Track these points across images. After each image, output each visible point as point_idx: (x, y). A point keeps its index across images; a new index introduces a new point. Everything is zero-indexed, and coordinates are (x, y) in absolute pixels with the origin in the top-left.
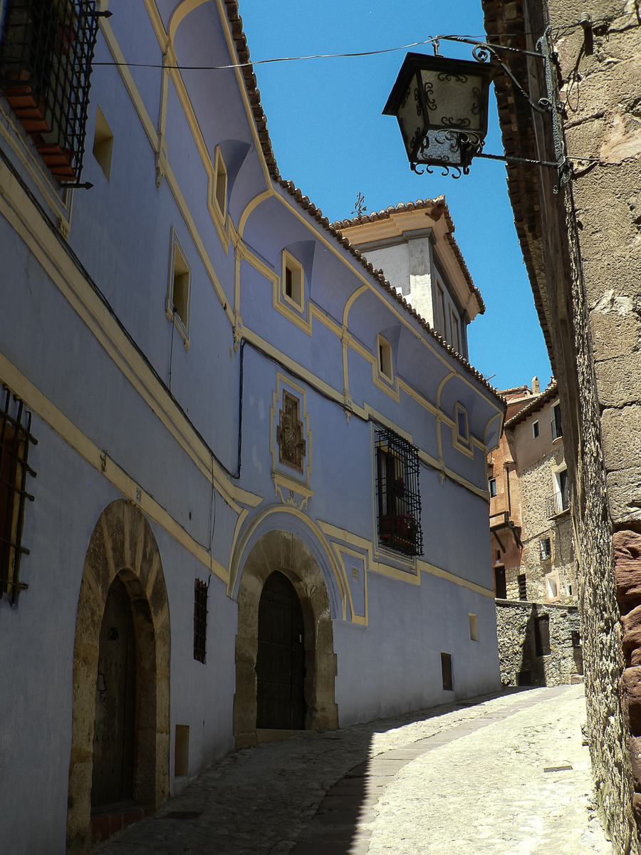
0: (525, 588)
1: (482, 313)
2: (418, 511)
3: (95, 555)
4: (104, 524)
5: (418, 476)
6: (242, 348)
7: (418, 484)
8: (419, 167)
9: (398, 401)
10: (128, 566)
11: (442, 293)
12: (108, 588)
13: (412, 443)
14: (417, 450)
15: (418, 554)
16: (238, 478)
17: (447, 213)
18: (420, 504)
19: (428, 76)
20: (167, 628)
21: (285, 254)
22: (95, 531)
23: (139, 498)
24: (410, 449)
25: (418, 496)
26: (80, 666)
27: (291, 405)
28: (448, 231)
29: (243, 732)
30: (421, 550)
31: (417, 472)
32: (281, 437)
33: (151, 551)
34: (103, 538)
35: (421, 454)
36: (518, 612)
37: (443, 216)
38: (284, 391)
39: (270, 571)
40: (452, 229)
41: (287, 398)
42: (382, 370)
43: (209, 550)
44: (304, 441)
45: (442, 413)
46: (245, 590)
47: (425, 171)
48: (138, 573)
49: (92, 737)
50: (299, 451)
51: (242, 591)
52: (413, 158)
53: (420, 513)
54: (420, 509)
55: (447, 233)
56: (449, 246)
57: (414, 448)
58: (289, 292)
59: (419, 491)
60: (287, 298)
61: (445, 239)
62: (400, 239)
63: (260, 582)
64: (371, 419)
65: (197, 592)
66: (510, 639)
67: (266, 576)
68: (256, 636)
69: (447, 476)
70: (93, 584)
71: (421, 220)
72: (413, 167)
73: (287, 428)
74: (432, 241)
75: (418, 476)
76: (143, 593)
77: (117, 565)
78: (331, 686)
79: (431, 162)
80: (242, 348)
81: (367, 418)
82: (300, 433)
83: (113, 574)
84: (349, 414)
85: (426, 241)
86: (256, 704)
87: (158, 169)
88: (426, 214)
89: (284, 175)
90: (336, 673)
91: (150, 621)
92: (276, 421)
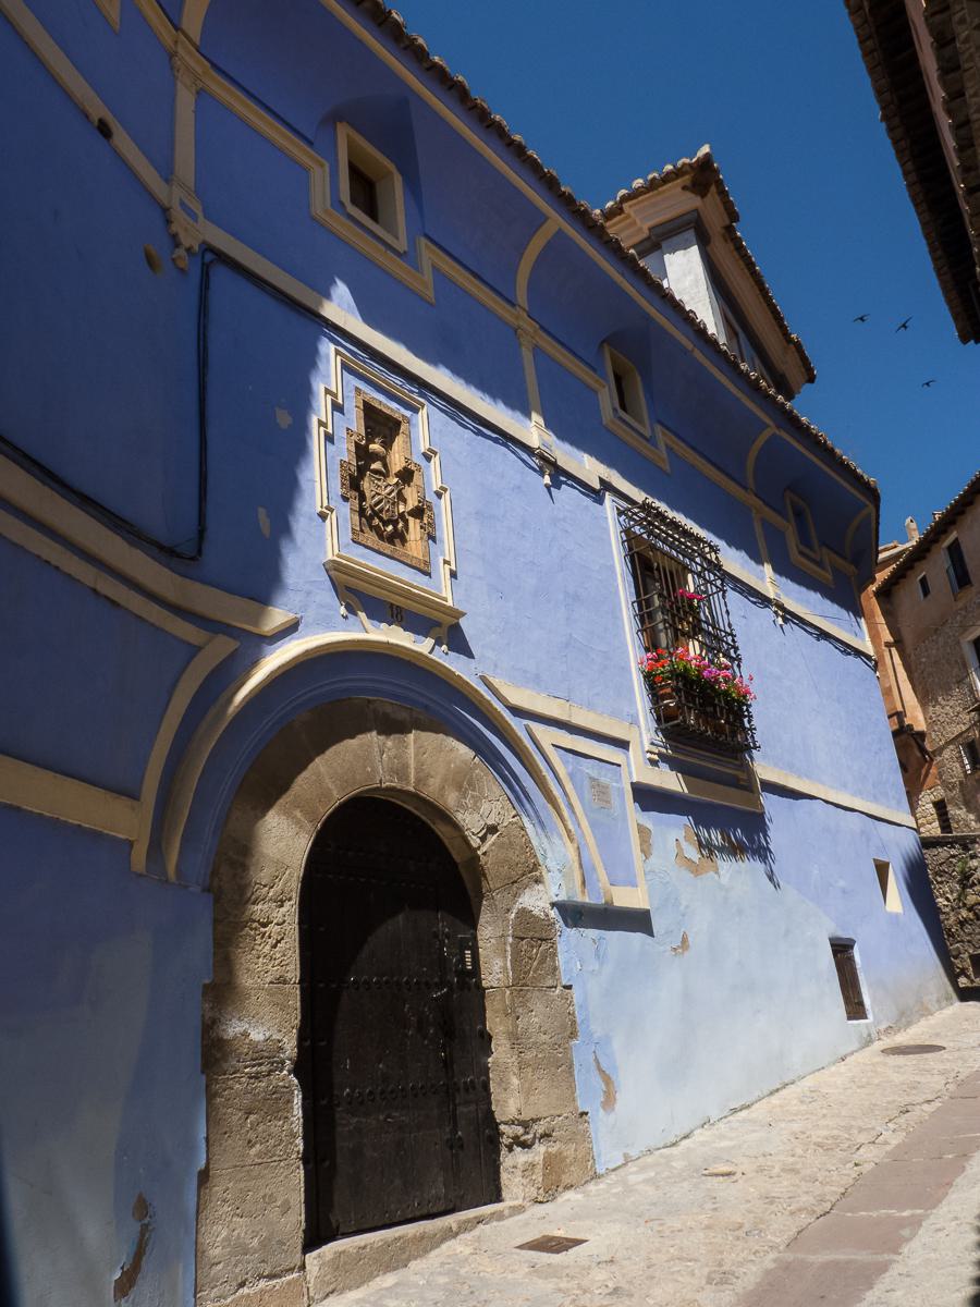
0: (948, 820)
1: (811, 379)
5: (724, 597)
7: (728, 612)
9: (667, 468)
11: (736, 334)
17: (719, 183)
18: (736, 649)
21: (343, 132)
25: (731, 634)
28: (727, 222)
29: (242, 1285)
30: (752, 737)
36: (953, 852)
37: (713, 189)
38: (358, 390)
42: (623, 407)
45: (761, 503)
56: (735, 253)
61: (726, 241)
63: (298, 822)
64: (607, 486)
66: (948, 899)
67: (326, 811)
68: (293, 972)
71: (677, 201)
74: (704, 242)
81: (597, 486)
88: (684, 188)
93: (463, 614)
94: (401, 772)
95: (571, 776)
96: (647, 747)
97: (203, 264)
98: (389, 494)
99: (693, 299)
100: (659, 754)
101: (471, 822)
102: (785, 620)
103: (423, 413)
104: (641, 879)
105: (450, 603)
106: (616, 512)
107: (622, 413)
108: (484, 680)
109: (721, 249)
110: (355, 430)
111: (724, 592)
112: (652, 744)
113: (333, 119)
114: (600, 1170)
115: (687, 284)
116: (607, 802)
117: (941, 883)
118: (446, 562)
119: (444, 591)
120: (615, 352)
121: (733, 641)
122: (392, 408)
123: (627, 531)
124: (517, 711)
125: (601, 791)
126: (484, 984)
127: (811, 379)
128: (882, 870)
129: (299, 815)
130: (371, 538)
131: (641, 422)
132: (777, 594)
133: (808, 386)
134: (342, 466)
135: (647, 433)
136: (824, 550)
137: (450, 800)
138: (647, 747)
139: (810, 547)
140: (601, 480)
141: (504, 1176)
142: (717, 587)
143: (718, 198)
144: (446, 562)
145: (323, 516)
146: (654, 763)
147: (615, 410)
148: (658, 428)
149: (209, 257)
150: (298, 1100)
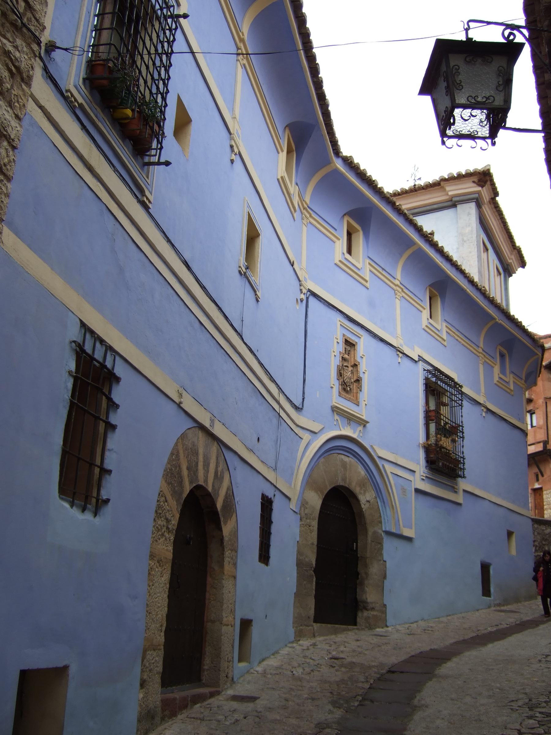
2: (461, 439)
3: (172, 474)
4: (180, 447)
6: (307, 298)
7: (462, 416)
8: (450, 142)
10: (201, 483)
11: (487, 250)
12: (182, 502)
13: (456, 380)
14: (461, 387)
15: (461, 477)
16: (302, 409)
18: (463, 433)
19: (455, 60)
20: (235, 533)
22: (172, 454)
23: (212, 425)
24: (456, 386)
26: (155, 567)
27: (349, 344)
28: (493, 196)
29: (301, 625)
30: (463, 473)
31: (461, 405)
32: (340, 374)
33: (222, 469)
34: (179, 460)
35: (465, 390)
37: (489, 183)
38: (344, 335)
39: (329, 488)
40: (496, 194)
41: (346, 341)
42: (431, 317)
43: (275, 470)
44: (361, 378)
46: (307, 503)
47: (455, 145)
48: (210, 489)
49: (164, 629)
50: (357, 386)
51: (304, 504)
52: (443, 134)
53: (463, 441)
54: (463, 437)
55: (492, 198)
57: (459, 385)
58: (349, 251)
59: (462, 422)
60: (347, 256)
61: (490, 204)
62: (450, 203)
63: (319, 495)
64: (421, 358)
65: (262, 504)
67: (326, 492)
68: (315, 543)
69: (489, 410)
70: (169, 497)
71: (470, 187)
72: (443, 143)
73: (346, 366)
74: (479, 206)
75: (461, 409)
76: (214, 505)
77: (191, 482)
78: (380, 588)
79: (461, 136)
80: (307, 298)
81: (417, 359)
82: (357, 371)
83: (187, 488)
84: (401, 355)
85: (473, 205)
86: (314, 600)
87: (232, 147)
88: (474, 182)
89: (345, 151)
90: (385, 577)
91: (220, 529)
92: (335, 362)
93: (367, 422)
94: (344, 480)
95: (395, 484)
96: (422, 474)
97: (307, 297)
98: (349, 375)
99: (468, 240)
100: (426, 477)
101: (363, 499)
102: (486, 412)
103: (362, 338)
104: (414, 528)
105: (364, 418)
106: (423, 369)
107: (430, 321)
108: (372, 446)
109: (487, 210)
110: (341, 352)
111: (462, 406)
112: (424, 473)
113: (345, 215)
114: (388, 624)
115: (467, 231)
116: (405, 495)
117: (544, 545)
118: (364, 401)
119: (362, 412)
120: (433, 290)
121: (462, 429)
122: (353, 338)
123: (427, 379)
124: (380, 458)
125: (404, 491)
126: (359, 555)
127: (523, 264)
128: (510, 534)
129: (319, 493)
130: (343, 393)
131: (436, 321)
132: (485, 402)
133: (520, 270)
134: (338, 367)
135: (439, 328)
136: (512, 375)
137: (357, 490)
138: (422, 474)
139: (505, 376)
140: (419, 356)
141: (358, 620)
142: (459, 404)
143: (490, 187)
144: (364, 401)
145: (332, 387)
146: (423, 479)
147: (428, 319)
148: (445, 324)
149: (309, 293)
150: (315, 579)
